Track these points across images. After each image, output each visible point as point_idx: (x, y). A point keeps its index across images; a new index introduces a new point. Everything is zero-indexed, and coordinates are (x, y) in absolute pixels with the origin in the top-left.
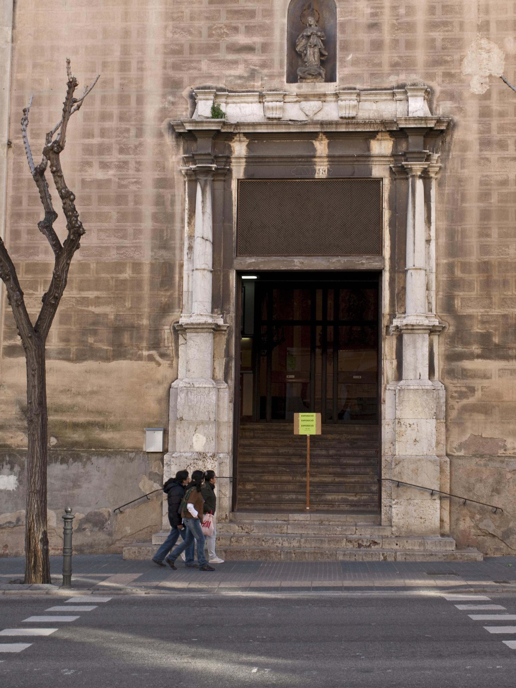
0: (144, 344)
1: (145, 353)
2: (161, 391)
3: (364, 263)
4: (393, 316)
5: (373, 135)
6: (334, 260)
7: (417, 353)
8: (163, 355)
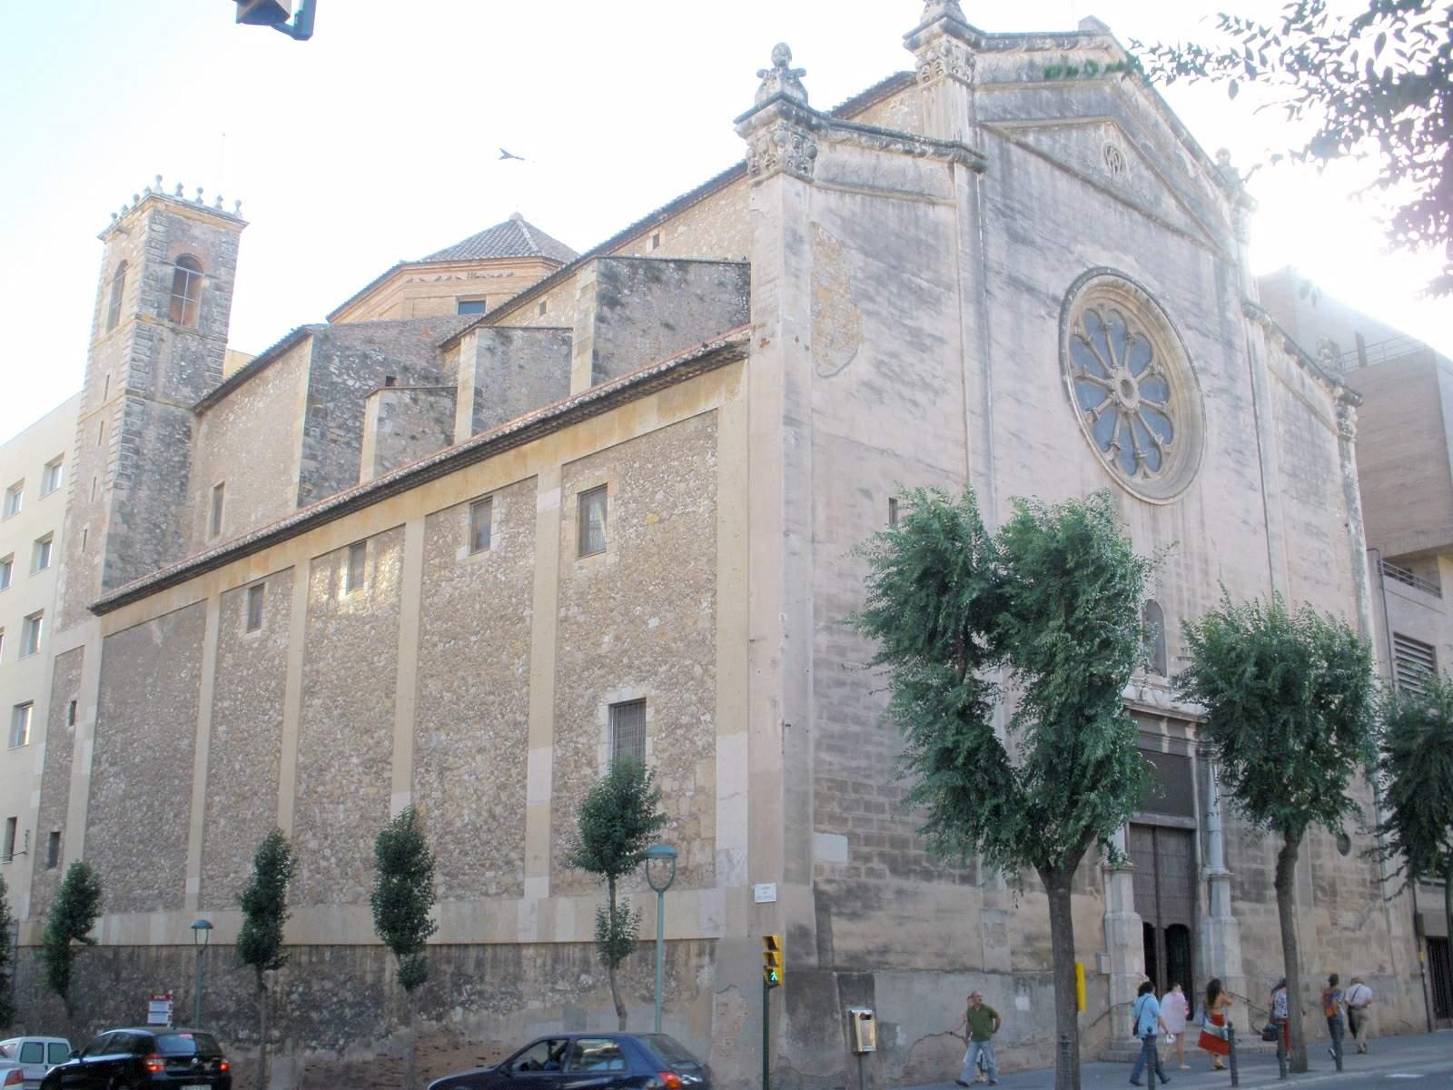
0: (1087, 881)
1: (1088, 889)
2: (1099, 922)
3: (1186, 822)
4: (1204, 866)
5: (1187, 723)
6: (1176, 818)
7: (1224, 893)
8: (1097, 891)
